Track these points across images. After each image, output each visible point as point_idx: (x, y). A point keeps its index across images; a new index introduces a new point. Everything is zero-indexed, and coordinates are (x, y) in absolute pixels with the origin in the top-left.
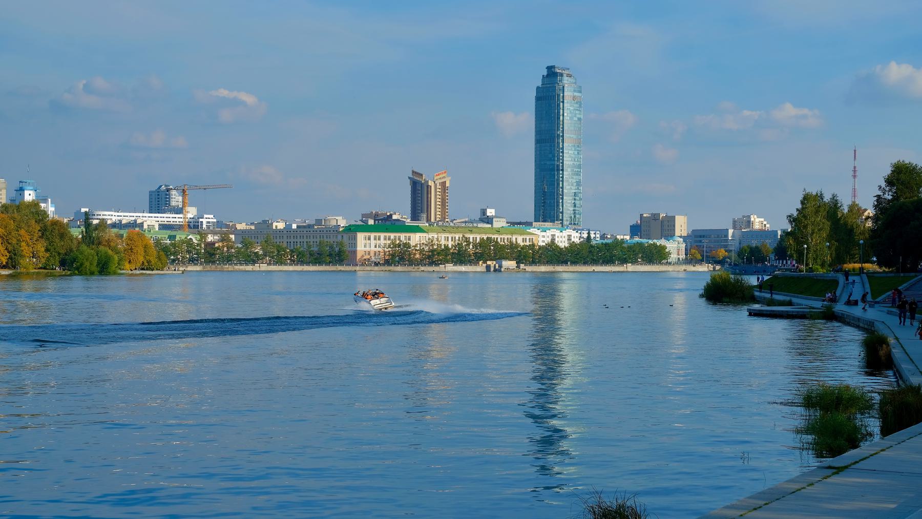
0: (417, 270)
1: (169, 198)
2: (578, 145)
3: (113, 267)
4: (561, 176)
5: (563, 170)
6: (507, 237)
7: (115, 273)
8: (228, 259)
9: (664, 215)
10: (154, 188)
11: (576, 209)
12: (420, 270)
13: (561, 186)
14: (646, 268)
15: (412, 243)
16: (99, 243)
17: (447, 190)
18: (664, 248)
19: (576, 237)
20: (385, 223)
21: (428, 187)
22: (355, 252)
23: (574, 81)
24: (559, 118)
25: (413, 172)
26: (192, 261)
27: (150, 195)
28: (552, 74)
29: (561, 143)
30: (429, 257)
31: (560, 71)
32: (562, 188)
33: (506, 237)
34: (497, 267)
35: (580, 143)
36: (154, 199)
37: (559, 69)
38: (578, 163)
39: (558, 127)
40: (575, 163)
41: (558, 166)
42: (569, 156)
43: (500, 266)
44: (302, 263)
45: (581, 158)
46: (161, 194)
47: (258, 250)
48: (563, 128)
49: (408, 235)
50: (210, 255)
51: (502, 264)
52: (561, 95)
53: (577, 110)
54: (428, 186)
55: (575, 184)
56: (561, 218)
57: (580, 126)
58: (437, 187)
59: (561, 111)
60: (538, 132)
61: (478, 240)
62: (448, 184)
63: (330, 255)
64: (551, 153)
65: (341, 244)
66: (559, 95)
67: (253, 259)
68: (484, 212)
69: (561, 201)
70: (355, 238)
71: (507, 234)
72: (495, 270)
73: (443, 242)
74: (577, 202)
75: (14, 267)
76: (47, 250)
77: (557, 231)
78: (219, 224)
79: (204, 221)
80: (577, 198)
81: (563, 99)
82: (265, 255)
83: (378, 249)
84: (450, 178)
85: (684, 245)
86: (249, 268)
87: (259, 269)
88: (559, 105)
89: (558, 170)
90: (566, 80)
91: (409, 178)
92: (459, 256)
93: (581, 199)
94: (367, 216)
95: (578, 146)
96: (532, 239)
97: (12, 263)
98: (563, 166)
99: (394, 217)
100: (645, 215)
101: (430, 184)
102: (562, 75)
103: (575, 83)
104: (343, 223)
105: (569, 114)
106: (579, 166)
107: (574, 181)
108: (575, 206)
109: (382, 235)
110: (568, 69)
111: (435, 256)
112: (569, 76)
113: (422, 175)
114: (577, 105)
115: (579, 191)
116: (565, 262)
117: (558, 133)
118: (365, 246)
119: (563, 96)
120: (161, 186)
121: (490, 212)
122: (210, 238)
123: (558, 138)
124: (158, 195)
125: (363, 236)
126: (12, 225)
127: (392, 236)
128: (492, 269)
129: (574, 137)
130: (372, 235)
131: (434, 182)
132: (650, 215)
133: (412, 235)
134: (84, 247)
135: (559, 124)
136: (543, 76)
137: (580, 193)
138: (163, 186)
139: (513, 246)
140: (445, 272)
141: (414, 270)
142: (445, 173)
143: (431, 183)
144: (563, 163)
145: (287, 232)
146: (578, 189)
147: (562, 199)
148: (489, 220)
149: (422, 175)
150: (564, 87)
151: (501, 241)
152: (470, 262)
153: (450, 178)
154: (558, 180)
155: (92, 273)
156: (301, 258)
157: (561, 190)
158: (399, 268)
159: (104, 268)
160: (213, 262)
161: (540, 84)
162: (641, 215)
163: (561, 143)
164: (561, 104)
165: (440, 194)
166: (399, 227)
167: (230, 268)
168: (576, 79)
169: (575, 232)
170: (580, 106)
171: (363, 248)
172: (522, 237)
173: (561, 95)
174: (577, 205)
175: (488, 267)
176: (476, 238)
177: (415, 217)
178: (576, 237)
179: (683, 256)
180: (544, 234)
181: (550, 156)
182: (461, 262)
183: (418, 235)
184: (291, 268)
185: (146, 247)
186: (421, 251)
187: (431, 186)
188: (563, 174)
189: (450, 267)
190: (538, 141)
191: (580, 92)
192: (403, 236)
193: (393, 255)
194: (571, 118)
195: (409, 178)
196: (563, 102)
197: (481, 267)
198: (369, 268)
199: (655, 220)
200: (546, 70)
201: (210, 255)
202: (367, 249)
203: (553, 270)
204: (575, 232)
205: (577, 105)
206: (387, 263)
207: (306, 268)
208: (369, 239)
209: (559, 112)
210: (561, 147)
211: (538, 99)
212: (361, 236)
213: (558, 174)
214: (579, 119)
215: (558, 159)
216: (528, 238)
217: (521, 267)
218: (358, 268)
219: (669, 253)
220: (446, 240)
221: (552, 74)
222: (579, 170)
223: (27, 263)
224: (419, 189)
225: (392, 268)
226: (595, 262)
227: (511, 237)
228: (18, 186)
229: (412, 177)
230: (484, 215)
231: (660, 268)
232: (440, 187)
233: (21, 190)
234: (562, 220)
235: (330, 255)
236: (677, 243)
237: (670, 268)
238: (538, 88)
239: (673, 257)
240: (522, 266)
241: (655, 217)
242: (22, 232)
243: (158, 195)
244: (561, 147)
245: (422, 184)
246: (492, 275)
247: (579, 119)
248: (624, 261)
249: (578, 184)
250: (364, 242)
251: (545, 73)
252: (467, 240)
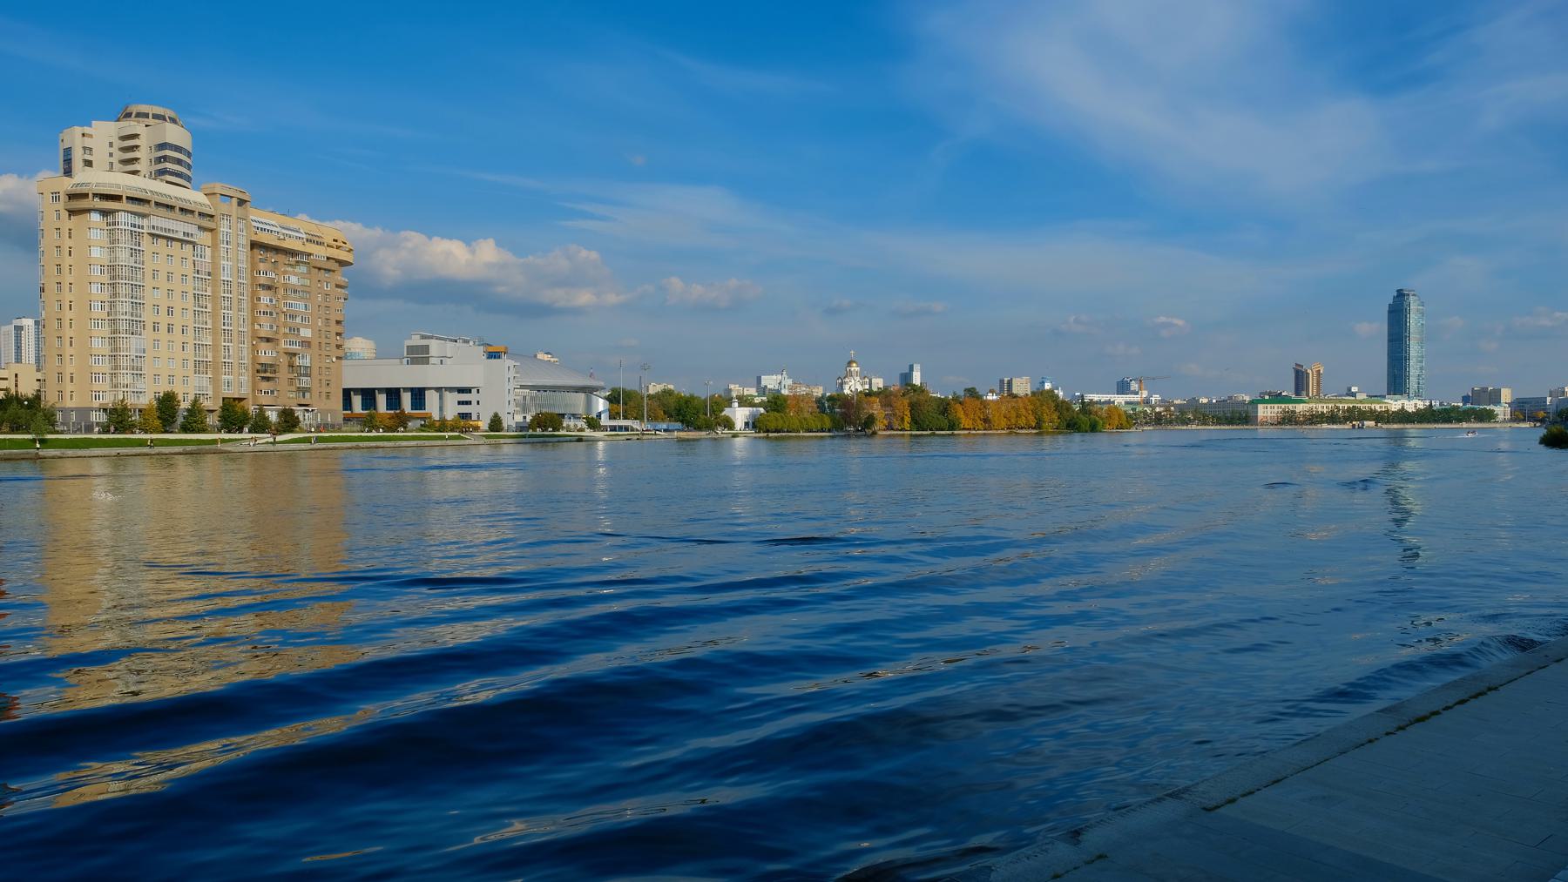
2: (1421, 342)
3: (1099, 428)
7: (1101, 432)
8: (1170, 422)
15: (1297, 411)
16: (1091, 413)
20: (1277, 398)
24: (1406, 324)
25: (1296, 364)
26: (1146, 423)
27: (1118, 385)
28: (1401, 295)
30: (1310, 419)
41: (1406, 357)
42: (1414, 350)
43: (1363, 425)
44: (1220, 424)
47: (1190, 416)
49: (1294, 405)
50: (1158, 420)
60: (1390, 334)
63: (1239, 419)
65: (1247, 412)
67: (1186, 422)
68: (1349, 389)
70: (1257, 408)
72: (1359, 428)
73: (1320, 409)
75: (1040, 428)
76: (1059, 418)
78: (1162, 401)
79: (1153, 399)
82: (1195, 419)
83: (1272, 415)
86: (1185, 427)
88: (1406, 316)
89: (1406, 360)
90: (1412, 298)
92: (1332, 418)
94: (1266, 393)
97: (1038, 426)
99: (1283, 394)
102: (1408, 295)
104: (1247, 399)
105: (1414, 321)
109: (1276, 406)
111: (1314, 419)
112: (1414, 295)
121: (1354, 389)
122: (1158, 409)
126: (1038, 404)
127: (1283, 406)
129: (1418, 336)
130: (1269, 406)
133: (1297, 405)
134: (1081, 416)
135: (1406, 328)
139: (1372, 412)
148: (1354, 395)
152: (1340, 423)
155: (1086, 432)
156: (1219, 421)
158: (1288, 427)
159: (1093, 428)
160: (1161, 424)
166: (1288, 400)
167: (1172, 428)
175: (1354, 426)
177: (1298, 393)
179: (1508, 417)
182: (1334, 423)
183: (1302, 405)
184: (1212, 428)
185: (1119, 415)
186: (1304, 415)
189: (1325, 426)
190: (1390, 341)
192: (1291, 406)
193: (1284, 419)
194: (1416, 324)
197: (1348, 426)
198: (1267, 427)
201: (1158, 420)
206: (1279, 423)
207: (1223, 427)
209: (1406, 321)
211: (1390, 312)
212: (1260, 406)
218: (1258, 427)
219: (1497, 415)
220: (1322, 408)
221: (1401, 295)
223: (1047, 425)
225: (1283, 427)
226: (1436, 421)
228: (1041, 380)
233: (1043, 383)
235: (1239, 419)
237: (1498, 425)
239: (1501, 417)
240: (1379, 424)
241: (1484, 390)
242: (1044, 407)
245: (1303, 372)
247: (1422, 324)
248: (1460, 421)
249: (1421, 368)
252: (1338, 408)
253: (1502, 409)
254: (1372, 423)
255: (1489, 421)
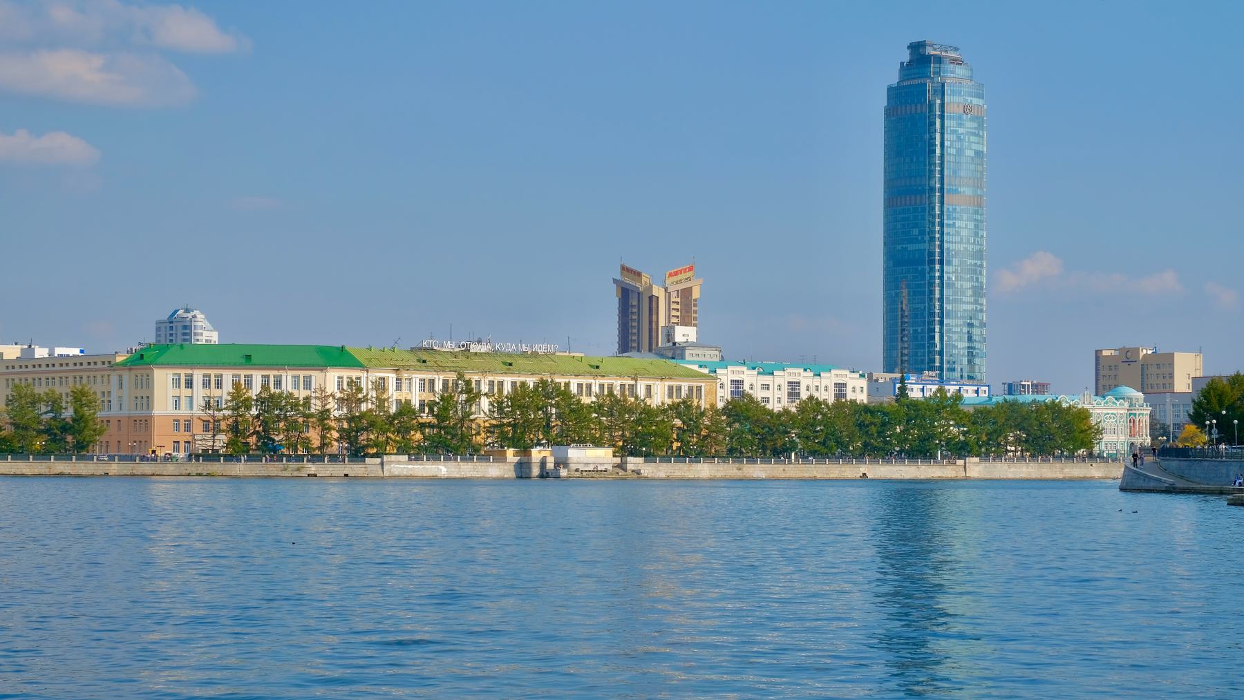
0: (295, 474)
1: (190, 334)
4: (937, 274)
5: (941, 262)
6: (619, 382)
9: (1150, 352)
10: (165, 317)
11: (975, 345)
12: (304, 473)
13: (937, 295)
14: (1024, 469)
17: (695, 305)
18: (1084, 415)
19: (858, 390)
21: (653, 300)
22: (144, 423)
23: (968, 73)
25: (623, 268)
27: (158, 329)
29: (937, 205)
31: (937, 53)
32: (941, 300)
33: (617, 383)
34: (550, 465)
35: (980, 205)
36: (163, 335)
37: (935, 50)
38: (976, 248)
39: (932, 172)
40: (970, 247)
41: (932, 254)
43: (562, 462)
45: (982, 236)
46: (176, 326)
48: (942, 172)
51: (567, 458)
52: (938, 102)
53: (974, 134)
54: (651, 298)
55: (970, 292)
56: (937, 364)
57: (980, 168)
58: (672, 300)
59: (938, 136)
61: (507, 389)
62: (696, 294)
64: (916, 226)
65: (79, 398)
66: (932, 105)
69: (937, 329)
70: (148, 383)
71: (620, 376)
72: (544, 475)
74: (975, 331)
77: (806, 374)
80: (975, 322)
81: (942, 111)
84: (700, 281)
85: (1147, 411)
87: (382, 475)
89: (932, 262)
91: (615, 281)
93: (983, 325)
95: (977, 212)
96: (699, 388)
98: (942, 253)
100: (1105, 353)
101: (655, 293)
103: (971, 78)
106: (979, 255)
107: (968, 285)
108: (970, 339)
110: (956, 49)
113: (639, 274)
114: (975, 125)
115: (979, 307)
116: (779, 452)
117: (932, 183)
118: (177, 405)
119: (942, 105)
120: (176, 311)
123: (931, 196)
124: (171, 328)
125: (171, 377)
128: (536, 471)
130: (198, 376)
131: (666, 290)
132: (1117, 353)
136: (902, 64)
137: (981, 311)
138: (181, 312)
140: (383, 478)
141: (286, 474)
142: (691, 269)
143: (658, 291)
144: (941, 247)
145: (7, 367)
146: (976, 302)
147: (941, 323)
149: (639, 274)
150: (943, 85)
151: (580, 392)
153: (700, 281)
154: (931, 284)
157: (937, 304)
161: (894, 79)
162: (1098, 352)
163: (937, 205)
164: (938, 121)
165: (678, 314)
168: (972, 70)
169: (857, 375)
170: (981, 127)
171: (171, 410)
172: (667, 383)
173: (938, 102)
174: (974, 338)
176: (501, 383)
178: (858, 390)
180: (767, 380)
181: (916, 232)
187: (658, 298)
188: (942, 271)
191: (980, 96)
195: (615, 281)
196: (942, 117)
199: (1128, 362)
200: (908, 52)
202: (184, 411)
203: (739, 474)
204: (857, 375)
205: (975, 125)
208: (190, 384)
210: (937, 212)
213: (932, 270)
214: (979, 154)
215: (932, 239)
216: (685, 386)
217: (630, 467)
222: (979, 262)
224: (635, 303)
227: (633, 382)
229: (618, 277)
230: (669, 341)
231: (1066, 470)
232: (678, 300)
234: (941, 369)
236: (1126, 405)
238: (890, 89)
240: (633, 462)
241: (1128, 356)
243: (171, 328)
244: (937, 212)
246: (536, 491)
247: (979, 154)
248: (960, 450)
250: (172, 392)
251: (906, 57)
253: (1122, 409)
254: (600, 457)
255: (1071, 457)
